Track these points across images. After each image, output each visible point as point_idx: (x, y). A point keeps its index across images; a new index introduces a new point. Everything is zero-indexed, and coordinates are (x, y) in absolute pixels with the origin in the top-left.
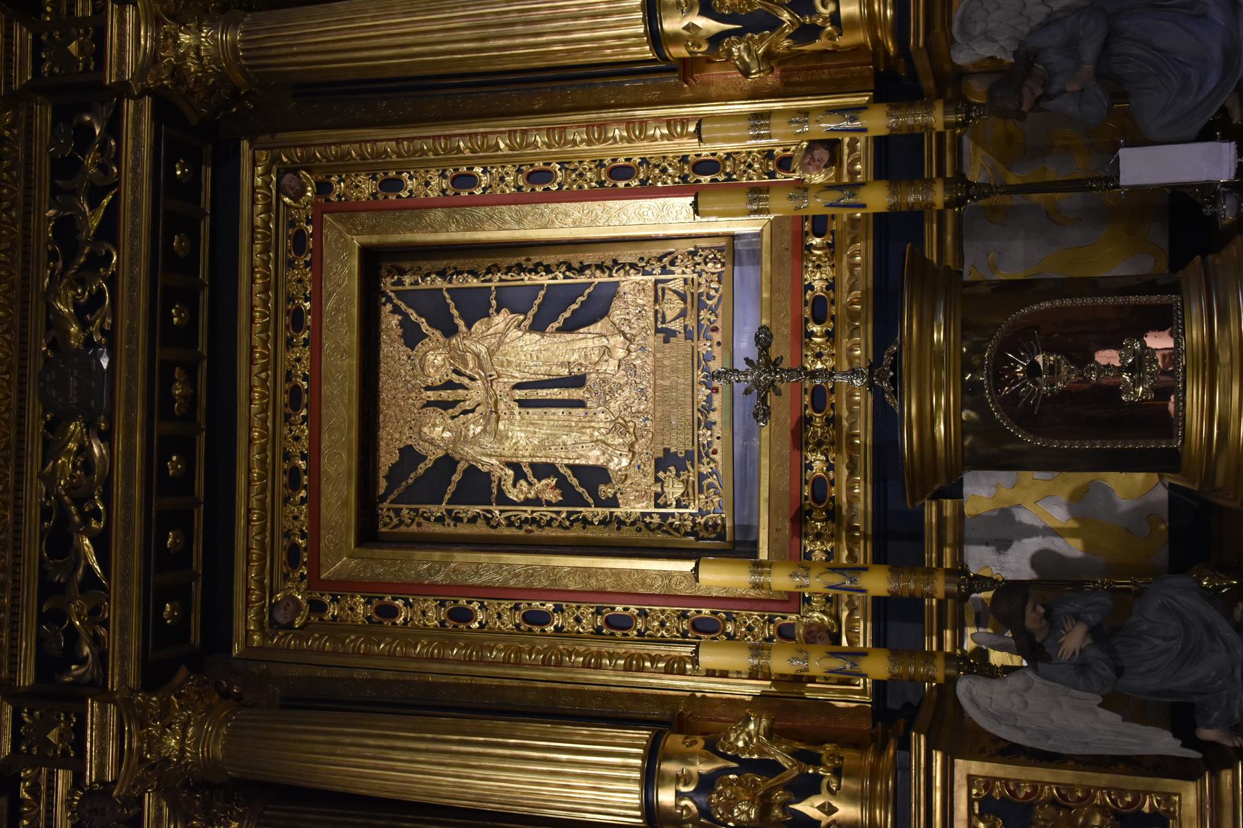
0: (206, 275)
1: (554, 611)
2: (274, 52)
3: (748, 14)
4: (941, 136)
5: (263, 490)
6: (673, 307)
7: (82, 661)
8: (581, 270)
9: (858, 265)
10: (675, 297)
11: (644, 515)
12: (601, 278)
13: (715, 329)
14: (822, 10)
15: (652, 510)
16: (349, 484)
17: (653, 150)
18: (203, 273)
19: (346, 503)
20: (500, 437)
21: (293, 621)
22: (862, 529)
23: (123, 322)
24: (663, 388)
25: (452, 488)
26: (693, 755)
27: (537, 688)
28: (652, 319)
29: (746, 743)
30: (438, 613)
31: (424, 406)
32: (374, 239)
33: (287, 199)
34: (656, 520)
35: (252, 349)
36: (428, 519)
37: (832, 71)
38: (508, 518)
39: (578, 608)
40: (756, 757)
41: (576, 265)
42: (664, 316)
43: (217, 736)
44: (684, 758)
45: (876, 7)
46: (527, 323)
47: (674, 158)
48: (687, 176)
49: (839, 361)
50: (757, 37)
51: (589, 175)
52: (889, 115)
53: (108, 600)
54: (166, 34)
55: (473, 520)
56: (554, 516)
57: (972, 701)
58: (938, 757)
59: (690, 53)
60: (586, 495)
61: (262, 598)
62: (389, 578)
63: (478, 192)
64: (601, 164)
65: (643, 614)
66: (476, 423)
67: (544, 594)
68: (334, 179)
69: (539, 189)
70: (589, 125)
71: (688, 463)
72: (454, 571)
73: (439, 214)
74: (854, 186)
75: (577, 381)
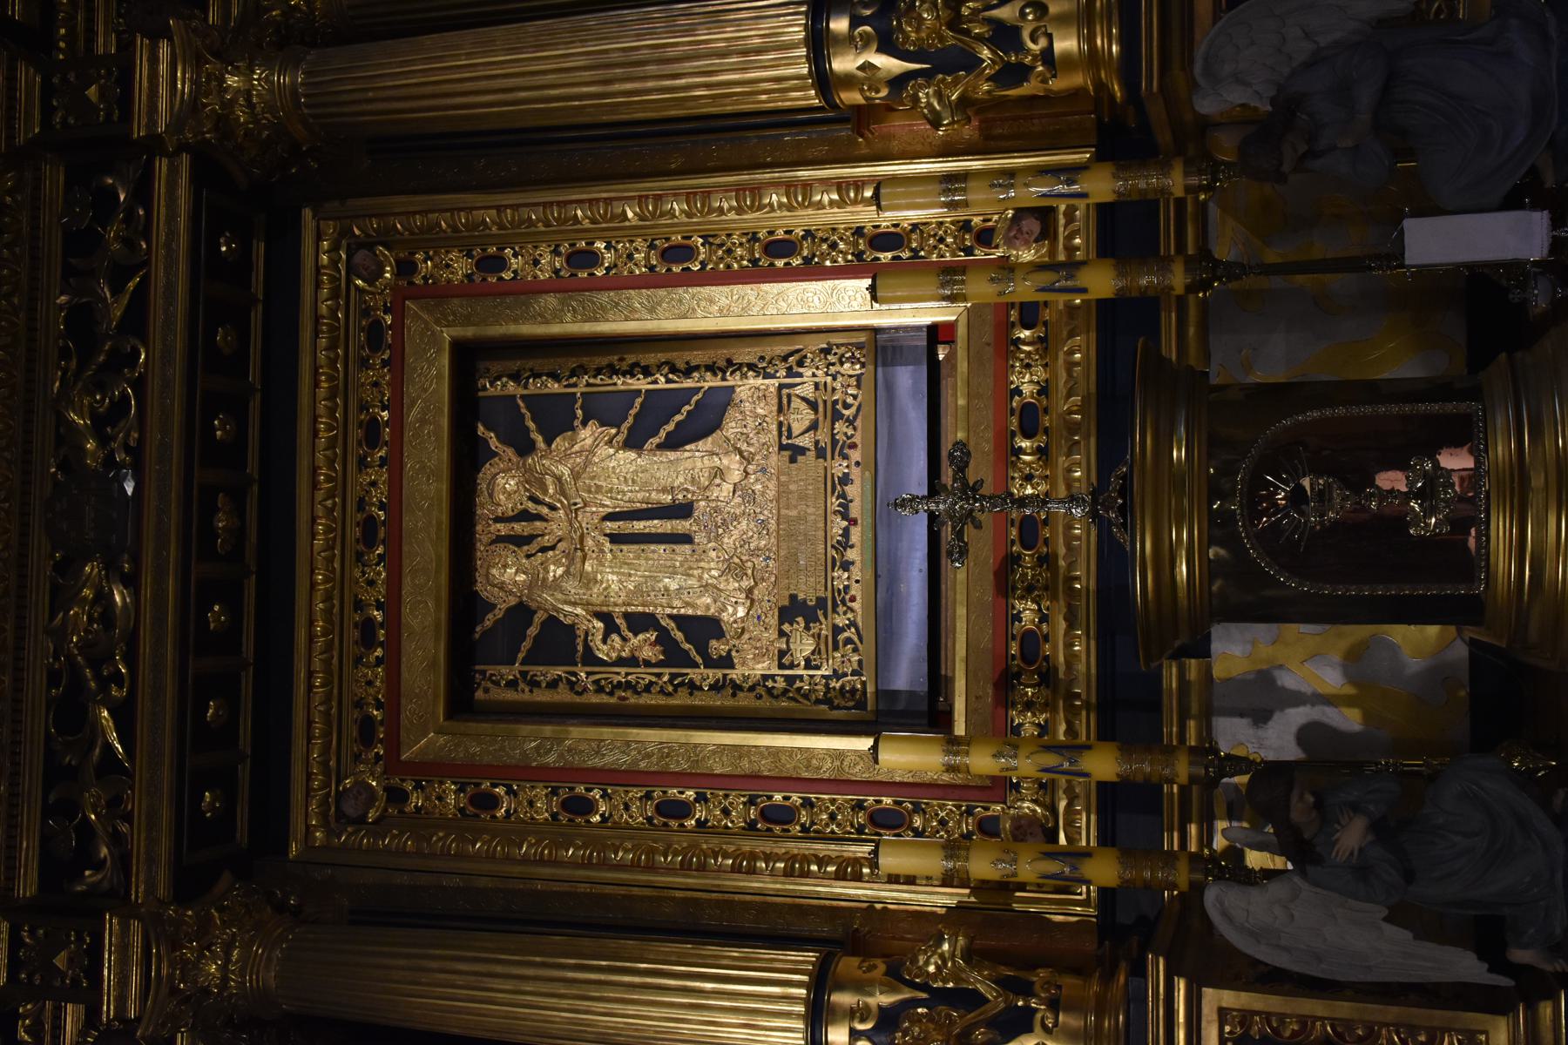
1: (696, 800)
2: (345, 97)
3: (938, 50)
4: (1180, 203)
6: (800, 418)
7: (98, 866)
8: (688, 372)
9: (1077, 364)
10: (803, 406)
11: (765, 677)
12: (711, 382)
13: (853, 446)
14: (1031, 45)
15: (775, 671)
18: (254, 375)
19: (433, 665)
20: (588, 581)
22: (1084, 696)
24: (789, 520)
25: (526, 645)
26: (871, 983)
27: (674, 898)
28: (775, 433)
29: (938, 967)
30: (549, 803)
31: (493, 542)
32: (469, 332)
33: (359, 282)
34: (781, 684)
35: (314, 471)
36: (497, 683)
38: (596, 682)
39: (726, 796)
40: (951, 985)
41: (681, 365)
42: (789, 429)
43: (269, 959)
44: (859, 987)
45: (1099, 42)
46: (620, 438)
47: (846, 229)
48: (863, 252)
49: (1054, 485)
50: (949, 79)
51: (739, 251)
52: (1116, 177)
53: (132, 788)
55: (553, 684)
56: (654, 679)
57: (1225, 914)
58: (1181, 986)
59: (866, 98)
60: (693, 653)
61: (326, 785)
62: (487, 759)
63: (600, 273)
64: (754, 238)
65: (808, 803)
66: (557, 563)
67: (683, 779)
69: (676, 269)
70: (739, 189)
71: (820, 613)
72: (570, 750)
73: (551, 301)
74: (1072, 266)
75: (683, 510)
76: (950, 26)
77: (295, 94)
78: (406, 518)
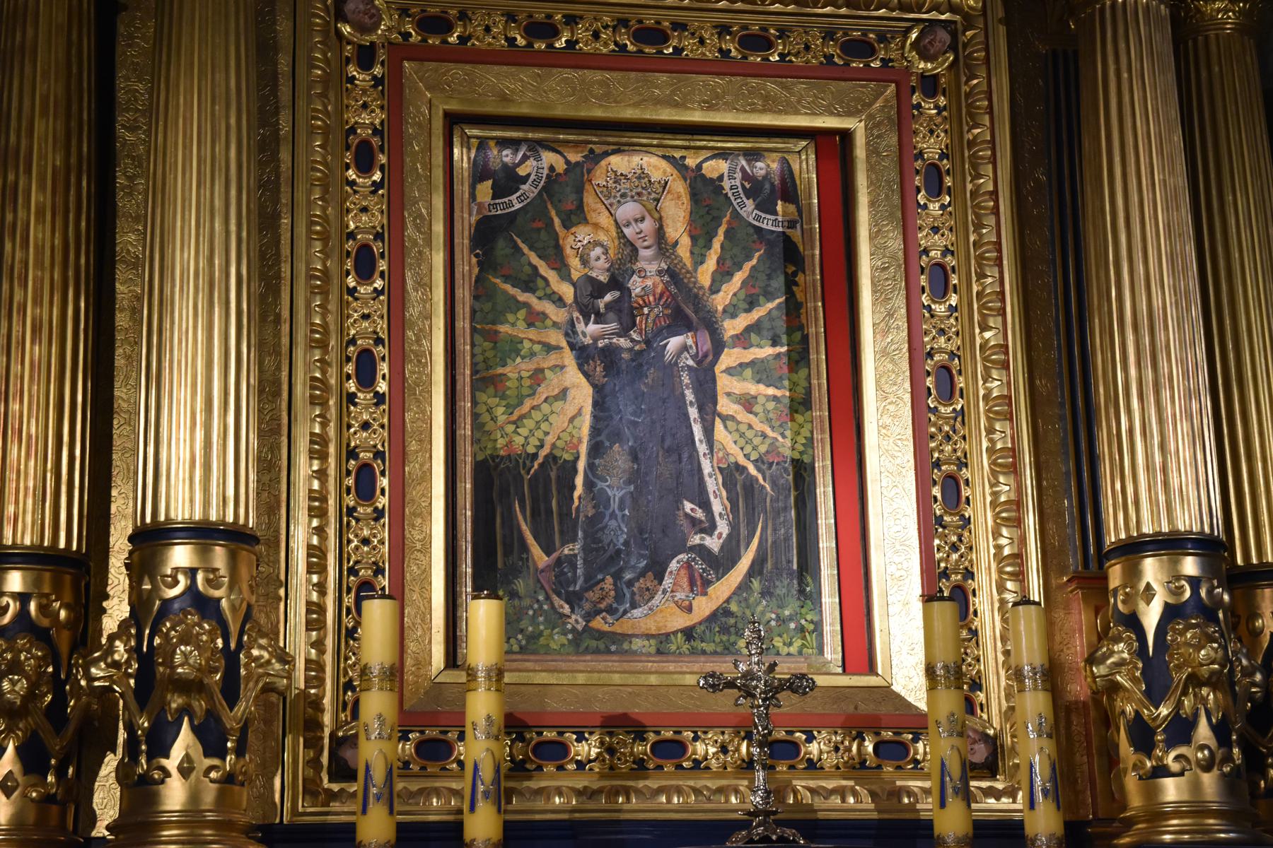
1: (377, 393)
2: (1122, 46)
3: (1167, 664)
9: (843, 801)
17: (981, 532)
19: (504, 99)
22: (509, 807)
27: (279, 369)
32: (860, 152)
37: (1086, 767)
39: (382, 426)
40: (243, 672)
45: (1175, 822)
47: (971, 561)
48: (948, 577)
49: (718, 776)
50: (1138, 674)
51: (948, 448)
52: (1051, 837)
59: (1115, 591)
63: (925, 299)
64: (962, 464)
68: (942, 101)
69: (929, 382)
70: (1014, 452)
72: (420, 253)
73: (895, 243)
76: (1190, 677)
78: (664, 77)
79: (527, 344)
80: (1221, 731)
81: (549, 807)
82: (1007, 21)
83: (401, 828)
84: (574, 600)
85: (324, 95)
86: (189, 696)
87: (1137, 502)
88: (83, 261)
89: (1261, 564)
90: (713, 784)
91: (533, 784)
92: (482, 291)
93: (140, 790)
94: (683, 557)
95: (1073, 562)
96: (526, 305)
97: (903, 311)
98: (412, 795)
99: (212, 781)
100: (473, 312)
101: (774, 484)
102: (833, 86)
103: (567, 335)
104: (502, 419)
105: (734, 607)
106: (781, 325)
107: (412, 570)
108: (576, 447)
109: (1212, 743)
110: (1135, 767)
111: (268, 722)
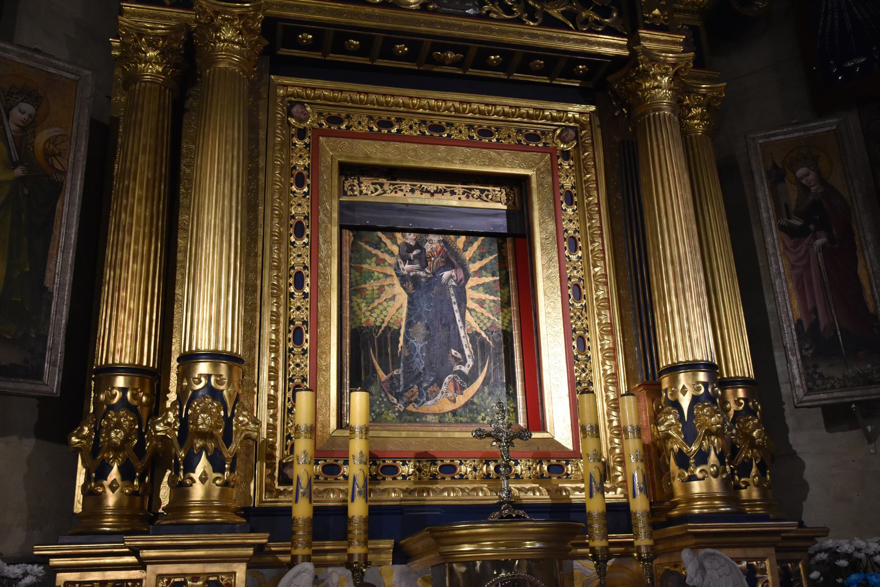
0: (517, 78)
1: (304, 293)
3: (695, 425)
5: (379, 103)
9: (534, 494)
16: (380, 159)
18: (517, 76)
19: (367, 157)
21: (292, 117)
23: (496, 26)
27: (256, 279)
29: (241, 422)
32: (534, 185)
33: (558, 132)
35: (469, 103)
40: (234, 428)
49: (472, 482)
51: (579, 323)
52: (643, 513)
54: (667, 69)
57: (299, 573)
58: (250, 551)
59: (666, 390)
61: (308, 97)
63: (567, 253)
69: (570, 292)
70: (611, 324)
73: (552, 227)
77: (660, 110)
78: (443, 148)
79: (376, 274)
80: (720, 457)
81: (390, 498)
82: (601, 126)
83: (315, 509)
84: (399, 396)
85: (280, 150)
86: (205, 440)
87: (676, 346)
88: (160, 224)
89: (728, 378)
90: (470, 486)
91: (381, 487)
92: (355, 249)
93: (181, 490)
94: (451, 376)
95: (641, 377)
96: (376, 255)
97: (557, 258)
98: (320, 492)
99: (217, 485)
100: (351, 258)
101: (494, 341)
102: (522, 154)
103: (395, 270)
104: (364, 309)
105: (475, 400)
106: (496, 267)
107: (321, 380)
108: (400, 323)
109: (718, 464)
110: (679, 476)
111: (248, 455)
